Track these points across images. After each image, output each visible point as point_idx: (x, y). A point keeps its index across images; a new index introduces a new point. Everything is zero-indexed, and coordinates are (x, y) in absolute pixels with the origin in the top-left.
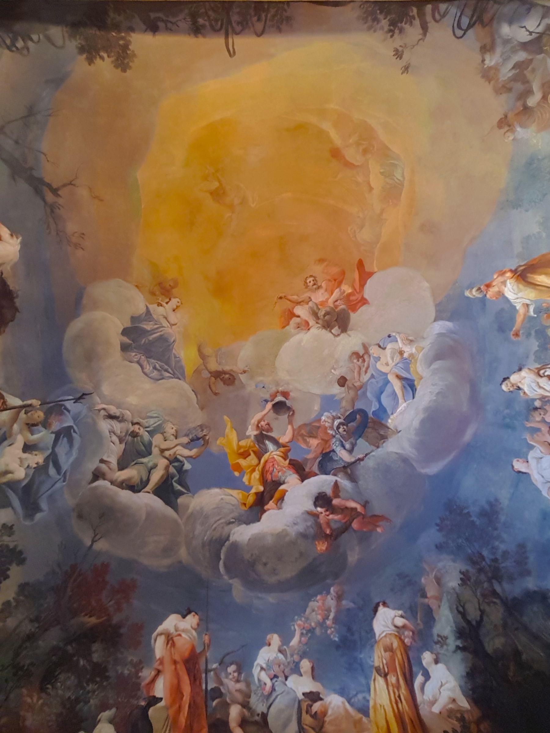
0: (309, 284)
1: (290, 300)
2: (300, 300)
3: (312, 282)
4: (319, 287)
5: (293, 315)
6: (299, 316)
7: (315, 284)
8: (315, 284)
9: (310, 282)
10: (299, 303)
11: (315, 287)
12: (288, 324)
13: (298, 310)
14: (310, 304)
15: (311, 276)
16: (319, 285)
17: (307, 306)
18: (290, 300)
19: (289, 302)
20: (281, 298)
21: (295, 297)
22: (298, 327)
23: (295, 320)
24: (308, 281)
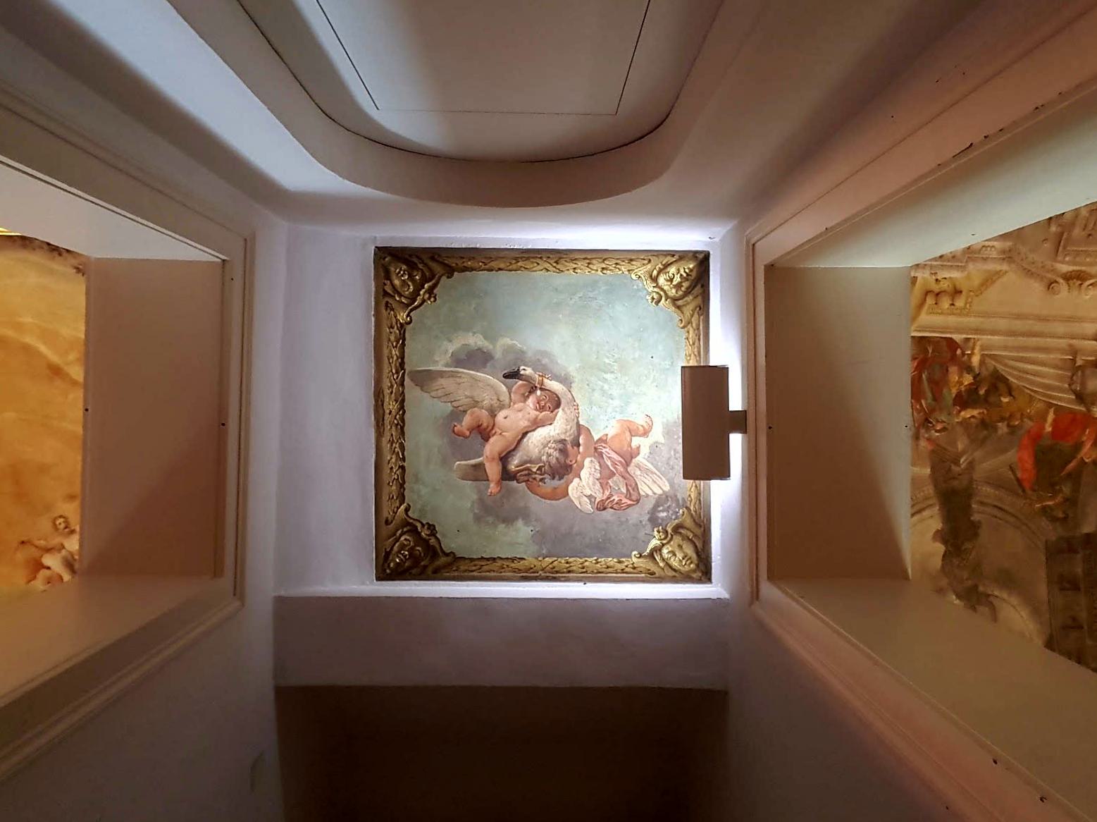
0: (59, 527)
1: (37, 547)
2: (49, 547)
3: (63, 526)
4: (73, 532)
5: (39, 566)
6: (49, 568)
7: (66, 528)
8: (66, 528)
9: (60, 524)
10: (48, 550)
11: (67, 530)
12: (35, 578)
13: (48, 560)
14: (64, 552)
15: (61, 517)
16: (73, 528)
17: (59, 555)
18: (37, 547)
19: (33, 549)
20: (23, 542)
21: (42, 543)
22: (49, 583)
23: (43, 573)
24: (57, 523)
